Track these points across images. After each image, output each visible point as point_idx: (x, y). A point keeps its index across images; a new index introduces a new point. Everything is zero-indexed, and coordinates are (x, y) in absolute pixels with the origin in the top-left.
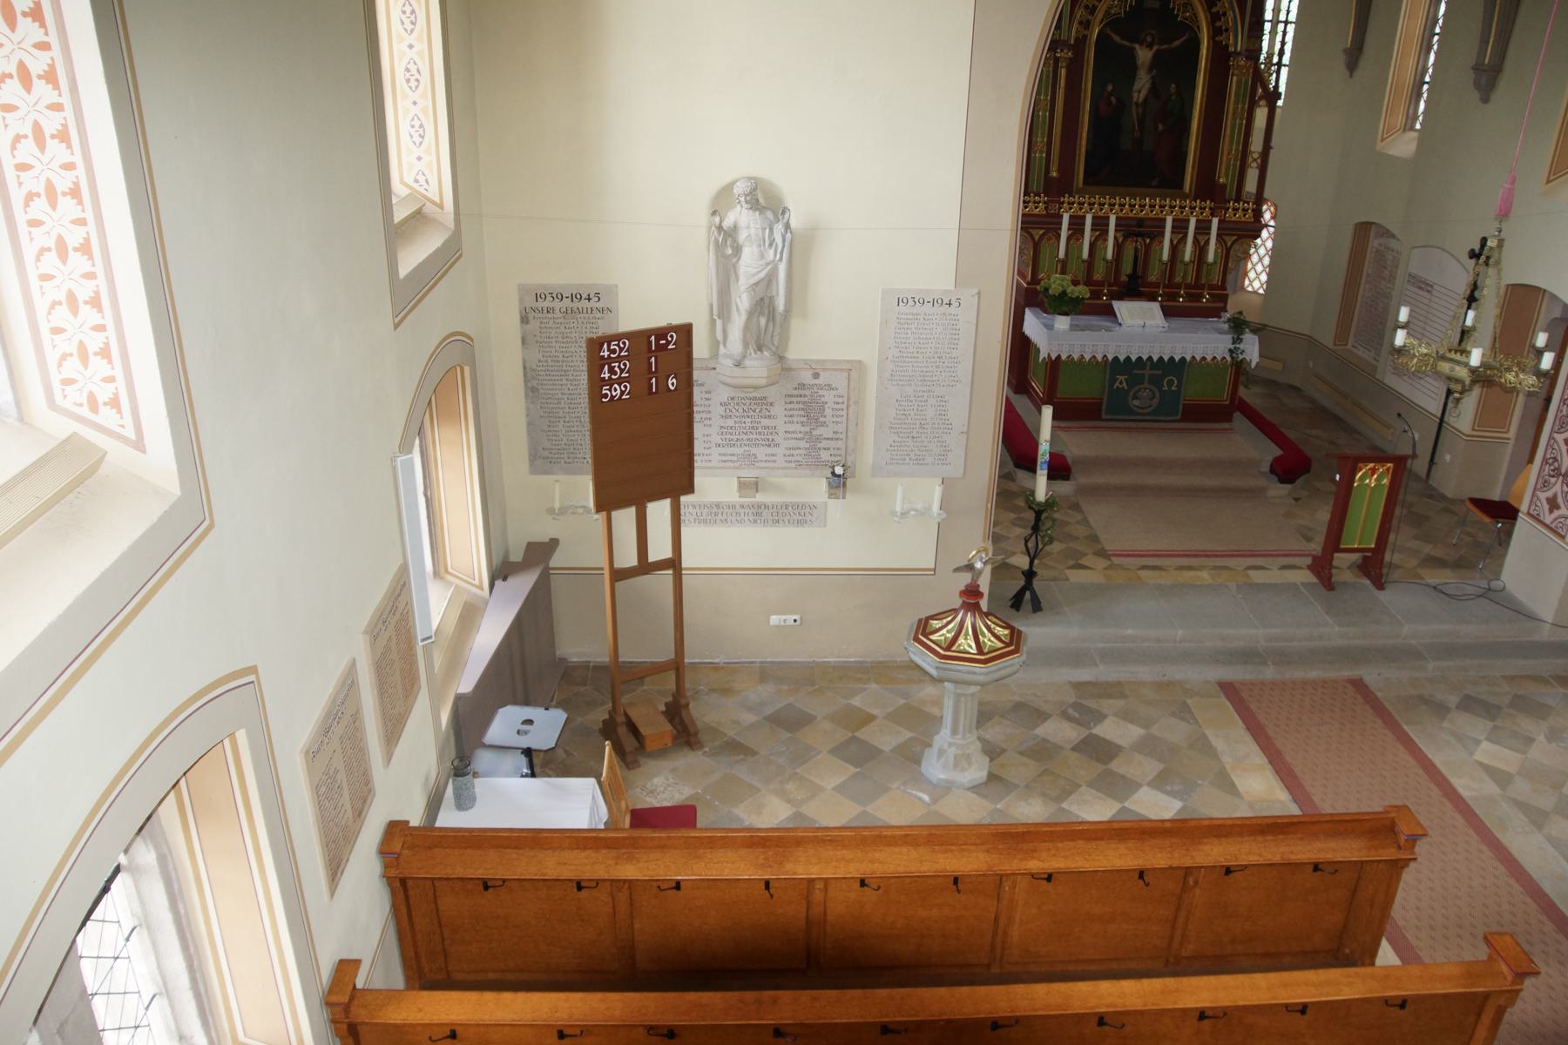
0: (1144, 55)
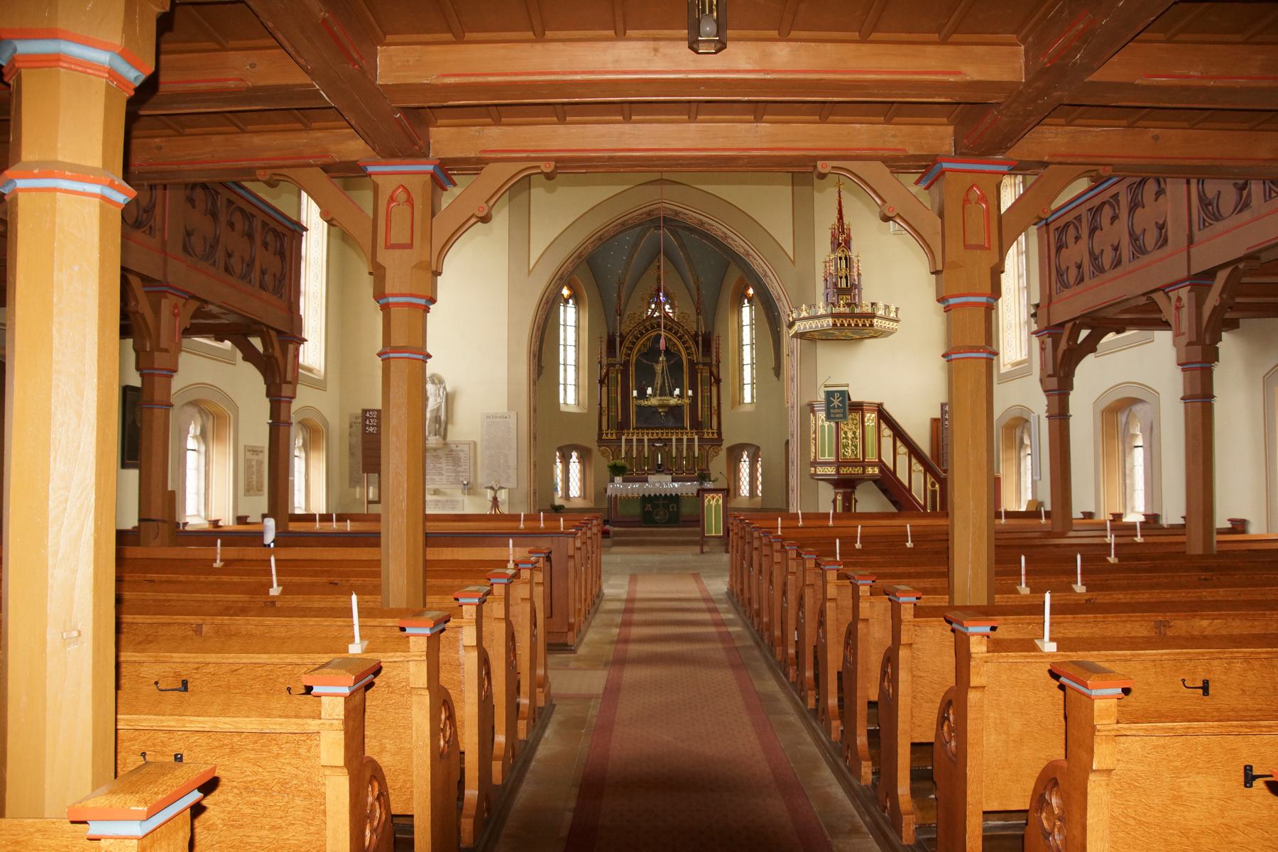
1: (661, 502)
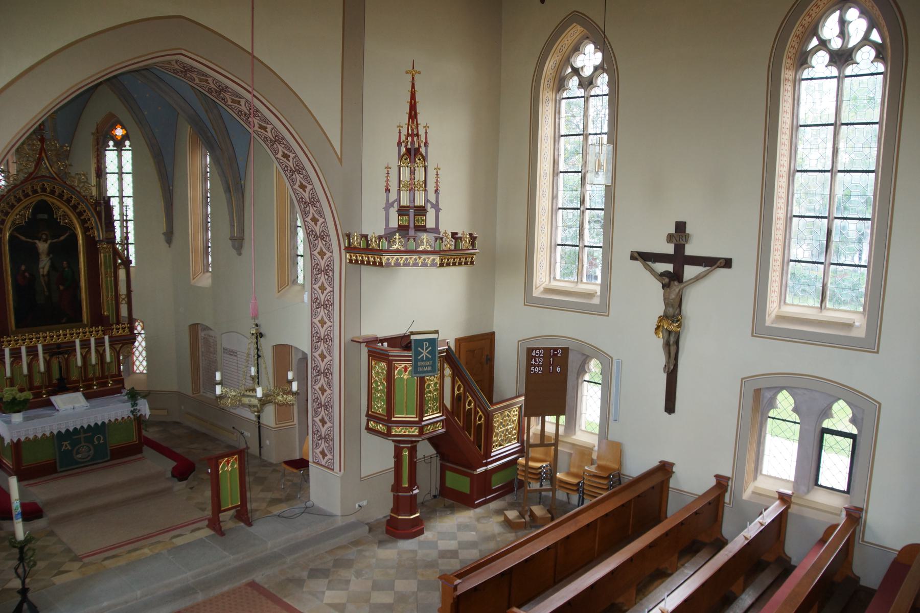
0: (43, 247)
1: (82, 436)
